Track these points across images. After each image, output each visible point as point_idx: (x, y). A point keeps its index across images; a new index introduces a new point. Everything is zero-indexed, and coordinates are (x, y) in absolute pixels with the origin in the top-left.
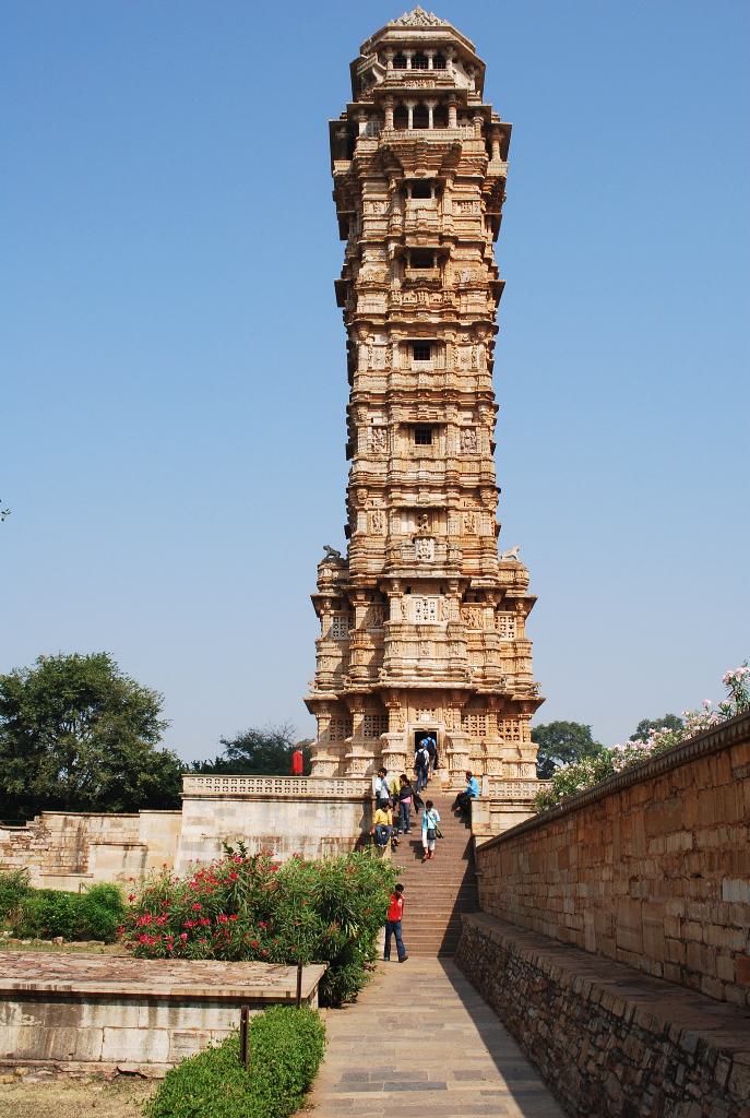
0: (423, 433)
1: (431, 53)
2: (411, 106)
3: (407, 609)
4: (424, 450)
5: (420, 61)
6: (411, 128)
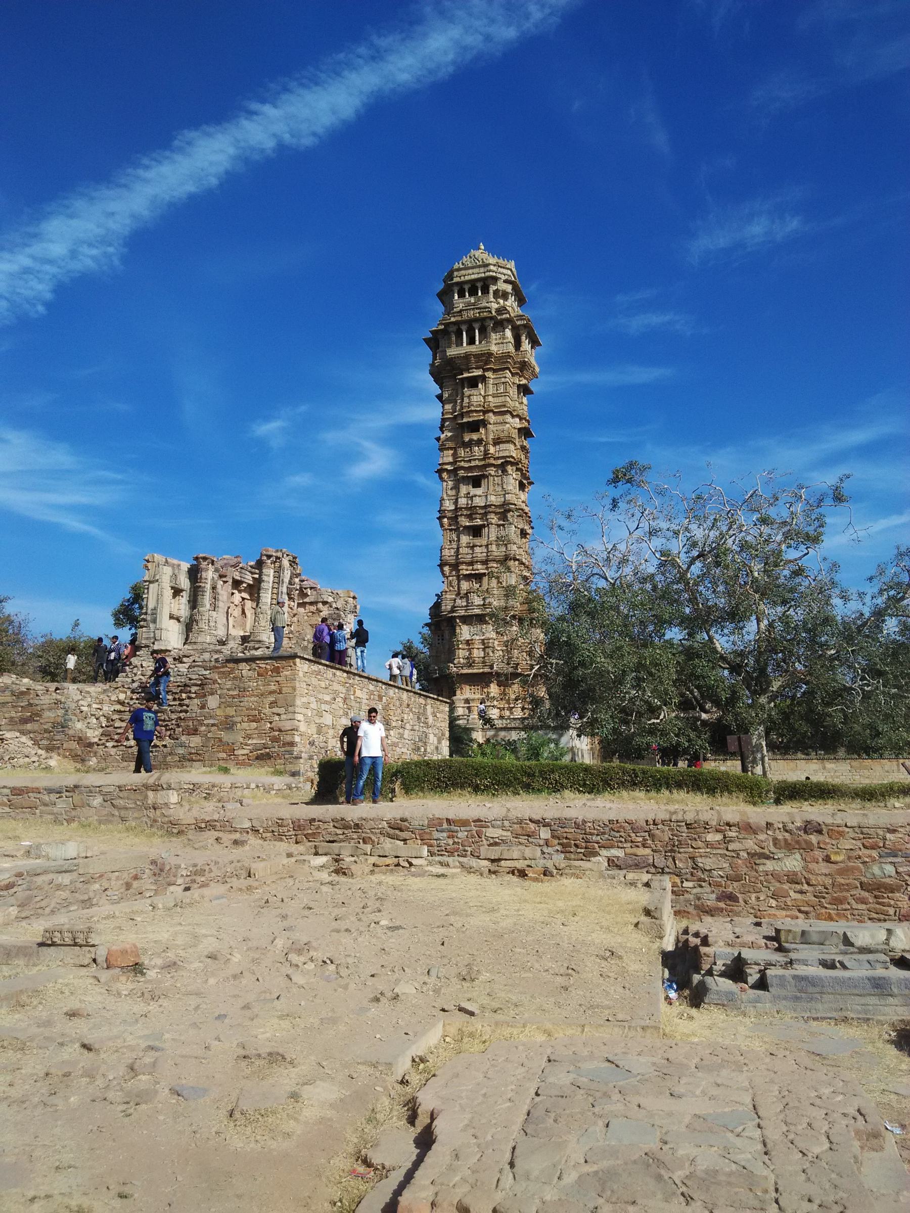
0: (476, 531)
1: (479, 285)
2: (464, 327)
3: (465, 632)
4: (477, 541)
5: (473, 292)
6: (465, 344)
